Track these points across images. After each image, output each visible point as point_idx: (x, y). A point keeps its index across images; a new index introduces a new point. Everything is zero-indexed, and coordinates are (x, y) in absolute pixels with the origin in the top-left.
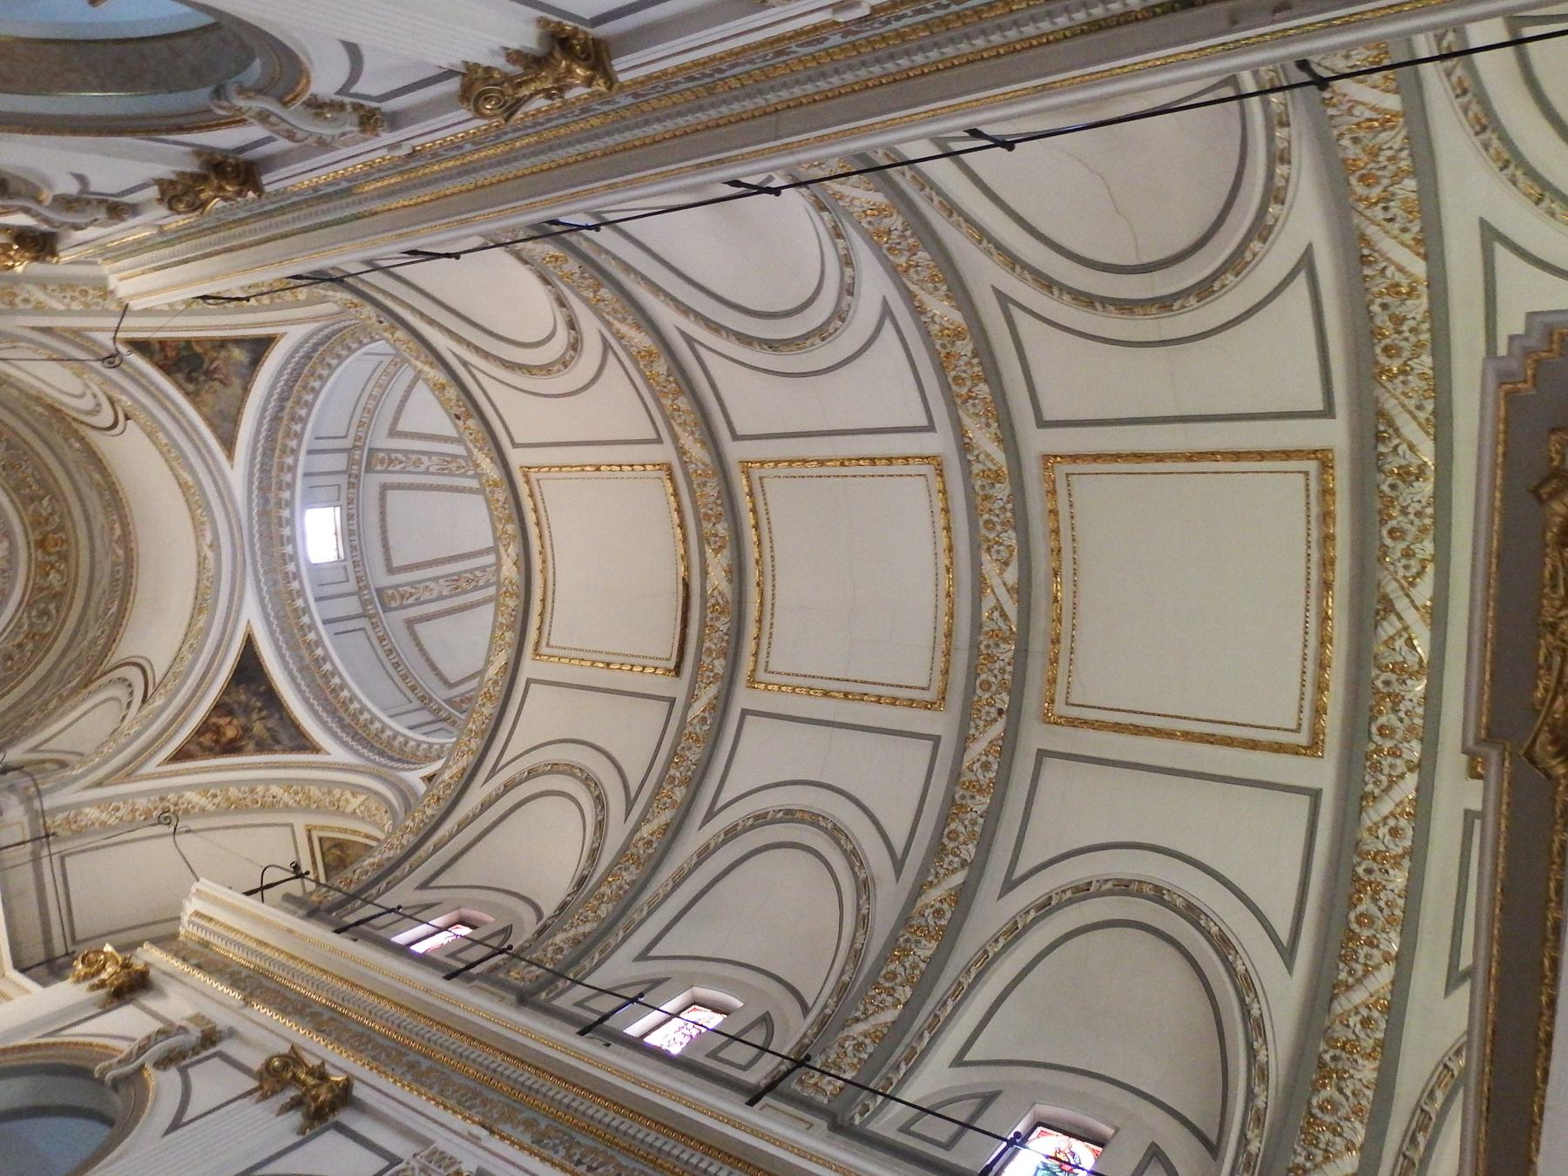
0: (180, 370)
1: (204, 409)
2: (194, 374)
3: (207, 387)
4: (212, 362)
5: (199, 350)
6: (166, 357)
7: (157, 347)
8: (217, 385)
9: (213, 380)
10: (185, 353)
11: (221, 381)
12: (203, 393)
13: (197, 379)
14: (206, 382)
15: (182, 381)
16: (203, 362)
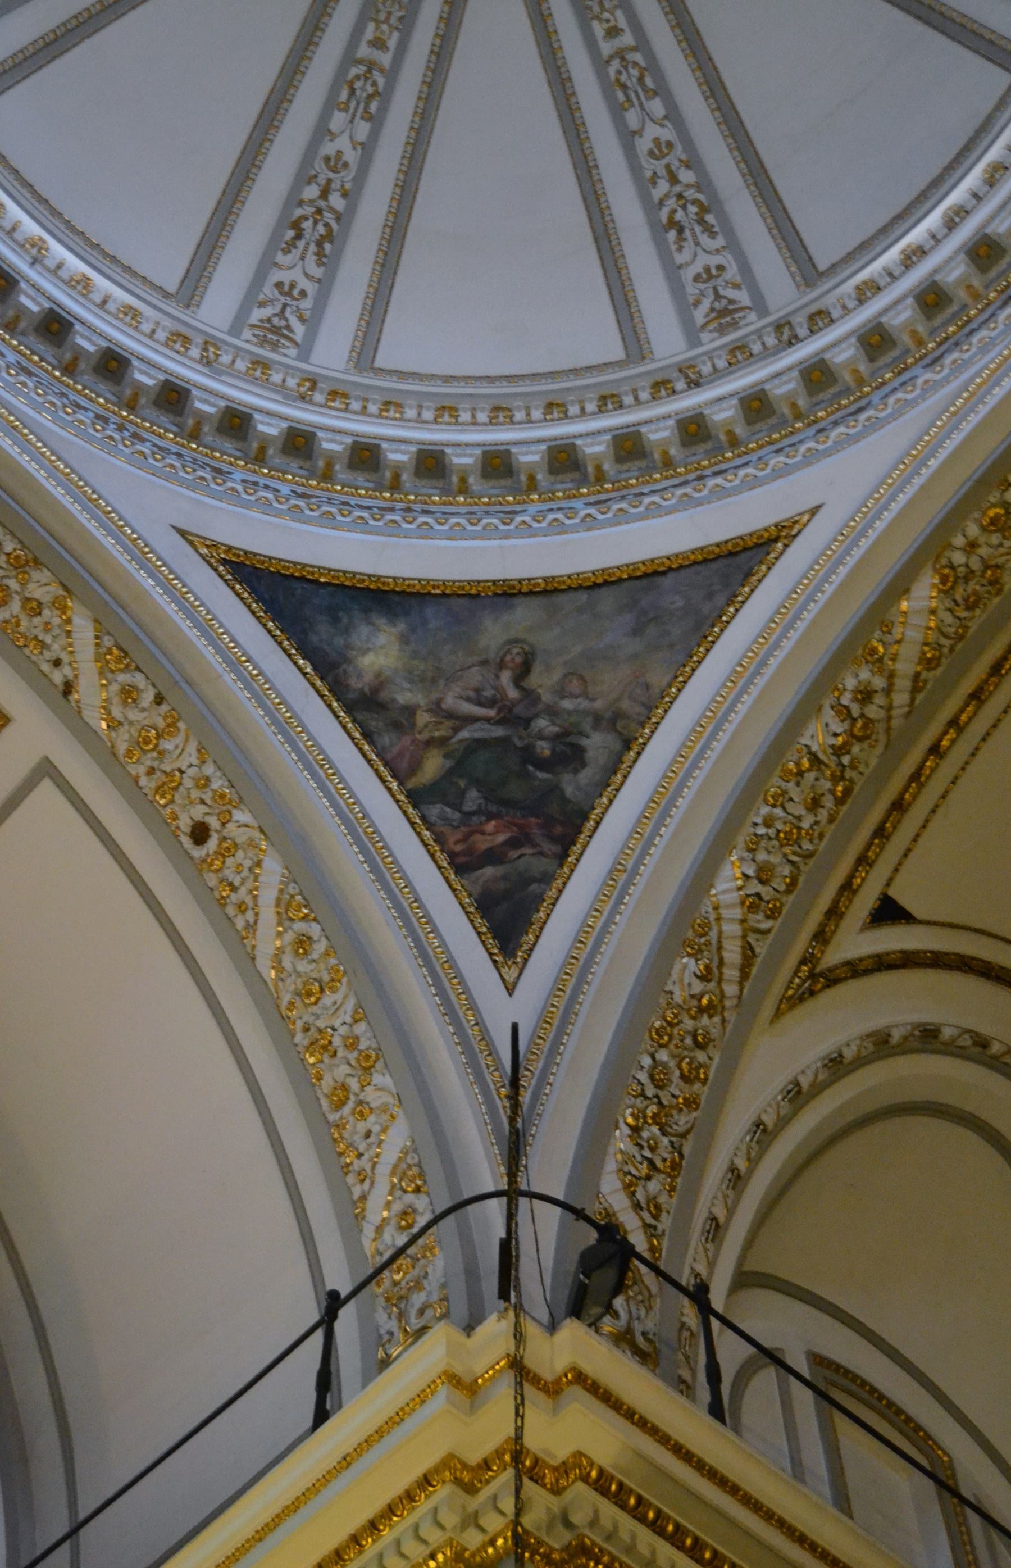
0: (555, 789)
1: (658, 678)
2: (544, 748)
3: (567, 704)
4: (470, 720)
5: (433, 766)
6: (514, 843)
7: (489, 871)
8: (542, 681)
9: (530, 696)
10: (473, 799)
11: (525, 669)
12: (598, 704)
13: (556, 738)
14: (552, 712)
15: (585, 776)
16: (481, 743)
